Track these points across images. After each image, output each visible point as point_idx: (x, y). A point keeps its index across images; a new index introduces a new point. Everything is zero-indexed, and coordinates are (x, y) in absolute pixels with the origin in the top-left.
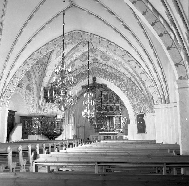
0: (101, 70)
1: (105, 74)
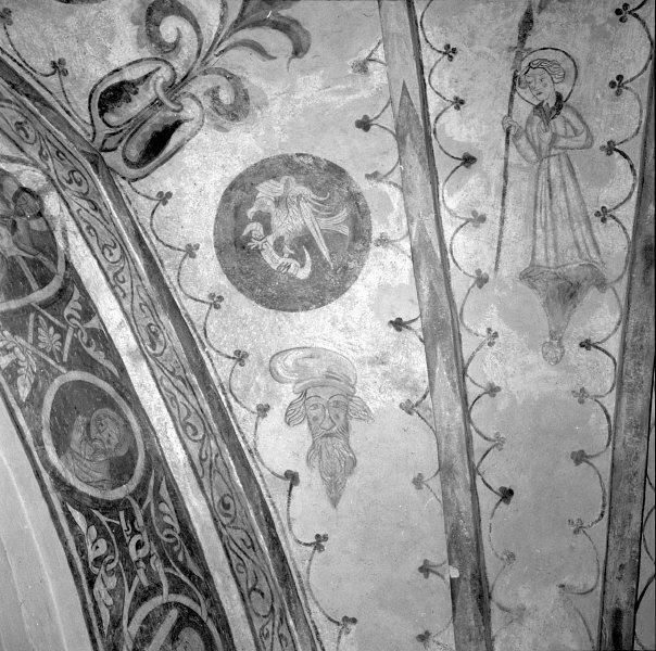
0: (63, 295)
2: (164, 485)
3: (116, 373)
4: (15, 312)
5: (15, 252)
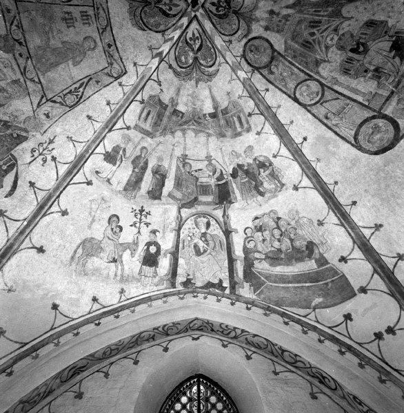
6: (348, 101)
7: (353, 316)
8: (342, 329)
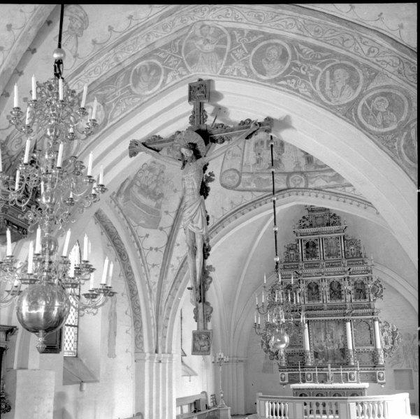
0: (233, 37)
1: (261, 54)
2: (300, 45)
3: (262, 36)
4: (227, 60)
5: (214, 46)
6: (241, 155)
7: (149, 236)
8: (141, 239)
